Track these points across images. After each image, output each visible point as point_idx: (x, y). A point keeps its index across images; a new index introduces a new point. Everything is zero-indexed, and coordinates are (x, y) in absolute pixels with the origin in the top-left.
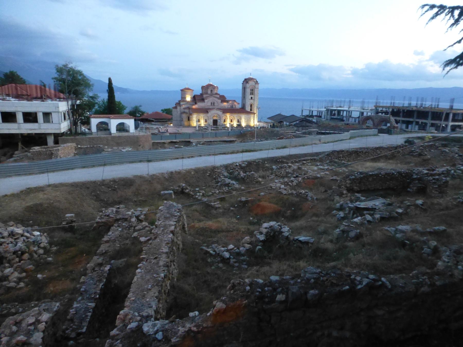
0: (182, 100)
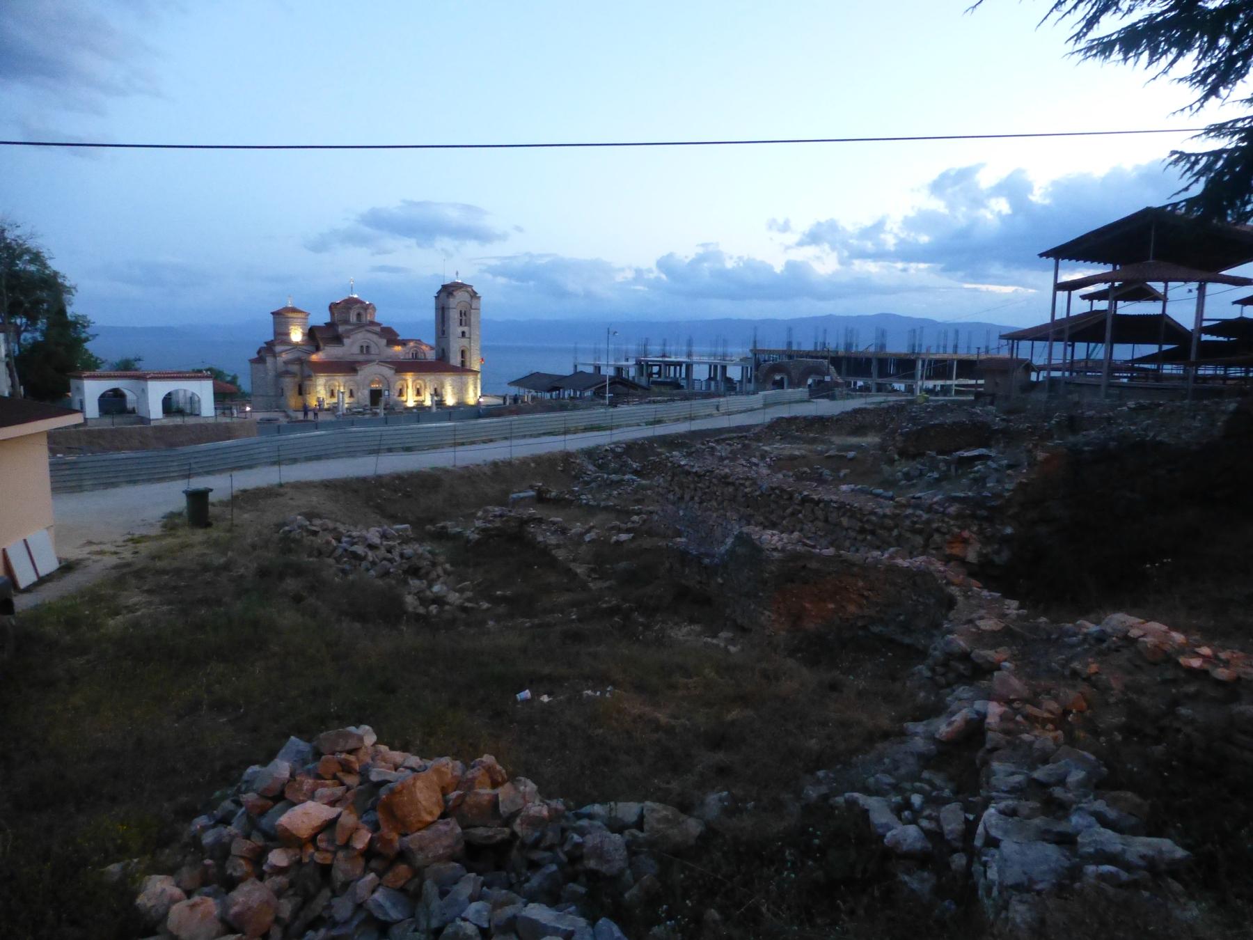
0: (275, 339)
